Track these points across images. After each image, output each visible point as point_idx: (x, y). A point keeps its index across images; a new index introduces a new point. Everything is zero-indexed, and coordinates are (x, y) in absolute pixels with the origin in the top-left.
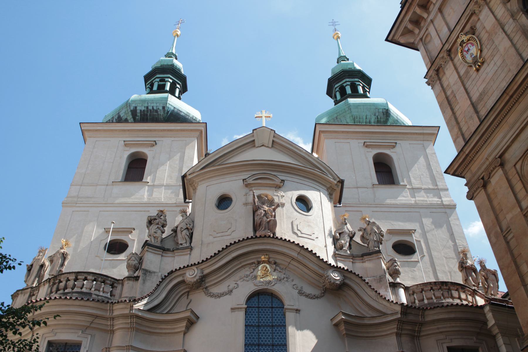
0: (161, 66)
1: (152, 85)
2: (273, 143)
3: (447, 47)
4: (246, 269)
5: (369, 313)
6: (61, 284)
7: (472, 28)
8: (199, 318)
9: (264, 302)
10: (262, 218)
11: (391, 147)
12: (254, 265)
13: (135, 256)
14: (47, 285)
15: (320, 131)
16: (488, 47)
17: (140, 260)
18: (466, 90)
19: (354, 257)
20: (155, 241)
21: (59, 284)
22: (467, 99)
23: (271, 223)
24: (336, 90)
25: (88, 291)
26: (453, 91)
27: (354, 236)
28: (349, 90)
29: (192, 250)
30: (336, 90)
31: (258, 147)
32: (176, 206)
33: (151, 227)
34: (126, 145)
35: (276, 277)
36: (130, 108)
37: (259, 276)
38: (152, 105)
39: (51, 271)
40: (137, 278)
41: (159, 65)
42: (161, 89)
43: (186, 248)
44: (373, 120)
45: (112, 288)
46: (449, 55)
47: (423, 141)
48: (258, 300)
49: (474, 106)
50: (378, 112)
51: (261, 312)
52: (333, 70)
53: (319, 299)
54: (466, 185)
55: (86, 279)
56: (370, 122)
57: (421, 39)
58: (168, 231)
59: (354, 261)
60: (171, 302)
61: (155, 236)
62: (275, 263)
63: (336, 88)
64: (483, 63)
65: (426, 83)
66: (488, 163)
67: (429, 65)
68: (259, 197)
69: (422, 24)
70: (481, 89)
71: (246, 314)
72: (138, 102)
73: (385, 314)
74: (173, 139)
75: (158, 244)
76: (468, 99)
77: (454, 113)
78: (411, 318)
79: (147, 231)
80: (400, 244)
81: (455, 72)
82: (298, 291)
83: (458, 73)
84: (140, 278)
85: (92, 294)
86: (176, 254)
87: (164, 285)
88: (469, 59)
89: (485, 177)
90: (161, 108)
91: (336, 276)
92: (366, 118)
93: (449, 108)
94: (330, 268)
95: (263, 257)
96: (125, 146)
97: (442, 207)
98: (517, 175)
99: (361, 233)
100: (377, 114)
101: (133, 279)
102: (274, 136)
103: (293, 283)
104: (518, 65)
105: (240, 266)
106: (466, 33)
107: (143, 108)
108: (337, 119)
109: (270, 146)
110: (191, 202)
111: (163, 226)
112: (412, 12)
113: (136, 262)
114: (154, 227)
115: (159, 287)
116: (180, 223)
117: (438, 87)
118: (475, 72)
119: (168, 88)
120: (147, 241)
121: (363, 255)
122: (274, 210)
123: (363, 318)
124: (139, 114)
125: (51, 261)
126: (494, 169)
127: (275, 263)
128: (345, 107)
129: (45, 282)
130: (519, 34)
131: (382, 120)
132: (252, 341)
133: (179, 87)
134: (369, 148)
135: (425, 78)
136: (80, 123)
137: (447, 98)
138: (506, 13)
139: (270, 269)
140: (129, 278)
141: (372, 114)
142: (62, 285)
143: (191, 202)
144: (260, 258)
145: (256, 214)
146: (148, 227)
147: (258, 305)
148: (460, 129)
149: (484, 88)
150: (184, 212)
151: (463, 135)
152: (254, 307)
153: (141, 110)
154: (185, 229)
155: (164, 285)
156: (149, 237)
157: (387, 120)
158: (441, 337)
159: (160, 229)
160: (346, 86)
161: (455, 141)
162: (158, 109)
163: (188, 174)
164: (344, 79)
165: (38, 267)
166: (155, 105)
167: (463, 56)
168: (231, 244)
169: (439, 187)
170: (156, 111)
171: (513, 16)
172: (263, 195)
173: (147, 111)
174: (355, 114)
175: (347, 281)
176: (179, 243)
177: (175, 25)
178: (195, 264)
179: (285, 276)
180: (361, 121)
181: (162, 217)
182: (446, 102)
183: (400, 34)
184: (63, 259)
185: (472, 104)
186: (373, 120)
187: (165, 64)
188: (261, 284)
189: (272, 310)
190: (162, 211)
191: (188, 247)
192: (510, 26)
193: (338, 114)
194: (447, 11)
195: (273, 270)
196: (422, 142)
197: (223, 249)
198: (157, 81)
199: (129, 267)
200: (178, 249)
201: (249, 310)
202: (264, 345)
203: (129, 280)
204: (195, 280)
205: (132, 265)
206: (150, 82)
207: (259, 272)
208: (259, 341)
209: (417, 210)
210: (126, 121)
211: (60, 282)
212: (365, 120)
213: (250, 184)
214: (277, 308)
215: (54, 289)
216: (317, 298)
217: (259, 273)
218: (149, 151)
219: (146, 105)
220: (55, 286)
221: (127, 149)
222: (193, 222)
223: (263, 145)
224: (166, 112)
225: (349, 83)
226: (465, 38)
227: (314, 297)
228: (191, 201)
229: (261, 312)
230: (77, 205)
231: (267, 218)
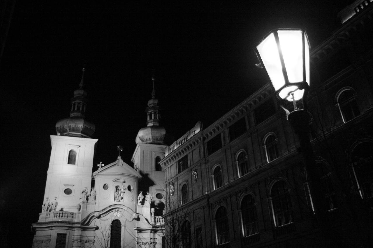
56: (158, 139)
62: (120, 211)
78: (154, 229)
90: (81, 127)
107: (73, 126)
109: (121, 165)
111: (87, 193)
114: (84, 193)
186: (159, 138)
207: (115, 214)
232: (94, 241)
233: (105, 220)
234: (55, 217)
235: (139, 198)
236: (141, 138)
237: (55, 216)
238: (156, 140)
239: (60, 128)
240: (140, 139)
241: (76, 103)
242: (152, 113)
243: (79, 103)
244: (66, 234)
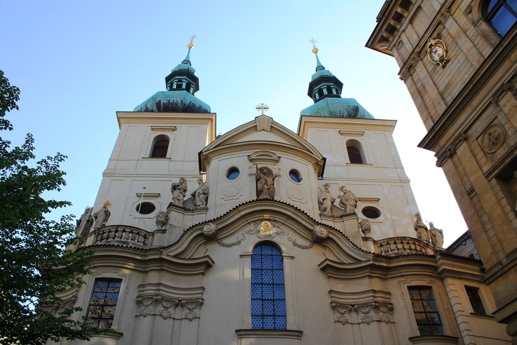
0: (179, 70)
1: (172, 84)
2: (271, 129)
3: (418, 50)
4: (252, 225)
5: (347, 260)
6: (104, 235)
7: (439, 34)
8: (214, 262)
9: (265, 251)
10: (264, 186)
11: (360, 135)
12: (258, 222)
13: (163, 214)
14: (93, 236)
15: (305, 121)
16: (453, 48)
17: (167, 217)
18: (434, 82)
19: (334, 217)
20: (178, 202)
21: (103, 235)
22: (435, 89)
23: (271, 189)
24: (316, 92)
25: (125, 240)
26: (422, 83)
27: (334, 201)
28: (325, 92)
29: (208, 210)
30: (316, 92)
31: (260, 131)
32: (193, 177)
33: (175, 192)
34: (152, 129)
35: (275, 232)
36: (155, 101)
37: (261, 231)
38: (173, 99)
39: (96, 224)
40: (165, 231)
41: (177, 69)
42: (179, 87)
43: (203, 209)
44: (345, 115)
45: (145, 238)
46: (419, 56)
47: (385, 131)
48: (261, 249)
49: (441, 95)
51: (263, 259)
52: (313, 76)
53: (309, 249)
54: (435, 156)
55: (124, 231)
57: (394, 45)
58: (188, 195)
59: (334, 221)
60: (192, 250)
61: (178, 198)
62: (275, 221)
63: (315, 90)
64: (448, 61)
65: (400, 78)
66: (454, 138)
67: (402, 65)
68: (261, 169)
69: (395, 34)
70: (446, 82)
71: (252, 260)
72: (162, 97)
73: (359, 261)
74: (190, 125)
75: (181, 205)
76: (436, 89)
77: (423, 101)
80: (367, 210)
81: (424, 68)
82: (292, 242)
83: (427, 70)
84: (167, 232)
85: (129, 242)
86: (195, 213)
87: (186, 236)
88: (437, 58)
89: (451, 149)
90: (180, 102)
92: (340, 113)
93: (419, 97)
94: (318, 225)
95: (265, 215)
96: (152, 130)
97: (400, 181)
98: (478, 146)
99: (339, 199)
100: (348, 110)
101: (161, 232)
102: (272, 123)
103: (289, 236)
104: (479, 61)
105: (247, 222)
106: (434, 38)
107: (166, 102)
108: (317, 113)
109: (269, 131)
110: (206, 174)
111: (185, 191)
112: (387, 24)
113: (164, 218)
114: (177, 192)
115: (182, 238)
116: (198, 189)
117: (409, 80)
118: (442, 69)
119: (184, 86)
120: (171, 203)
121: (342, 217)
122: (273, 179)
123: (343, 264)
125: (96, 218)
126: (459, 142)
127: (275, 221)
128: (324, 104)
129: (92, 233)
130: (479, 37)
131: (352, 115)
132: (257, 281)
133: (193, 86)
134: (343, 135)
135: (398, 74)
136: (116, 112)
137: (418, 89)
138: (468, 22)
139: (270, 226)
140: (158, 231)
141: (345, 109)
142: (105, 235)
143: (206, 174)
144: (263, 217)
145: (259, 182)
146: (172, 192)
147: (261, 253)
148: (429, 113)
149: (449, 81)
150: (201, 180)
151: (431, 117)
152: (258, 255)
153: (164, 103)
154: (202, 194)
155: (186, 236)
156: (173, 200)
157: (356, 115)
158: (402, 279)
159: (182, 194)
160: (323, 88)
161: (425, 122)
162: (178, 102)
163: (203, 151)
164: (322, 83)
165: (85, 222)
166: (175, 99)
167: (431, 56)
168: (240, 205)
169: (397, 167)
170: (176, 104)
171: (475, 24)
172: (264, 167)
173: (169, 104)
174: (331, 109)
175: (330, 236)
176: (197, 205)
178: (211, 221)
179: (282, 230)
180: (336, 115)
181: (183, 184)
182: (417, 93)
183: (377, 41)
184: (105, 215)
185: (439, 93)
186: (345, 115)
187: (182, 68)
188: (263, 237)
189: (272, 257)
191: (204, 207)
192: (472, 31)
193: (318, 109)
194: (416, 22)
195: (272, 226)
196: (383, 132)
197: (233, 209)
198: (176, 82)
199: (158, 222)
200: (196, 209)
201: (254, 257)
202: (266, 284)
203: (159, 232)
204: (212, 233)
205: (160, 221)
206: (170, 83)
208: (262, 281)
209: (381, 184)
210: (152, 111)
211: (104, 233)
212: (339, 114)
213: (253, 159)
214: (276, 255)
216: (307, 248)
217: (262, 228)
218: (171, 134)
219: (168, 99)
220: (100, 237)
221: (154, 132)
223: (263, 130)
224: (184, 105)
226: (433, 42)
227: (305, 247)
228: (205, 173)
229: (263, 259)
230: (115, 175)
231: (267, 186)
232: (203, 300)
233: (233, 244)
235: (324, 200)
242: (322, 88)
243: (180, 81)
244: (120, 281)
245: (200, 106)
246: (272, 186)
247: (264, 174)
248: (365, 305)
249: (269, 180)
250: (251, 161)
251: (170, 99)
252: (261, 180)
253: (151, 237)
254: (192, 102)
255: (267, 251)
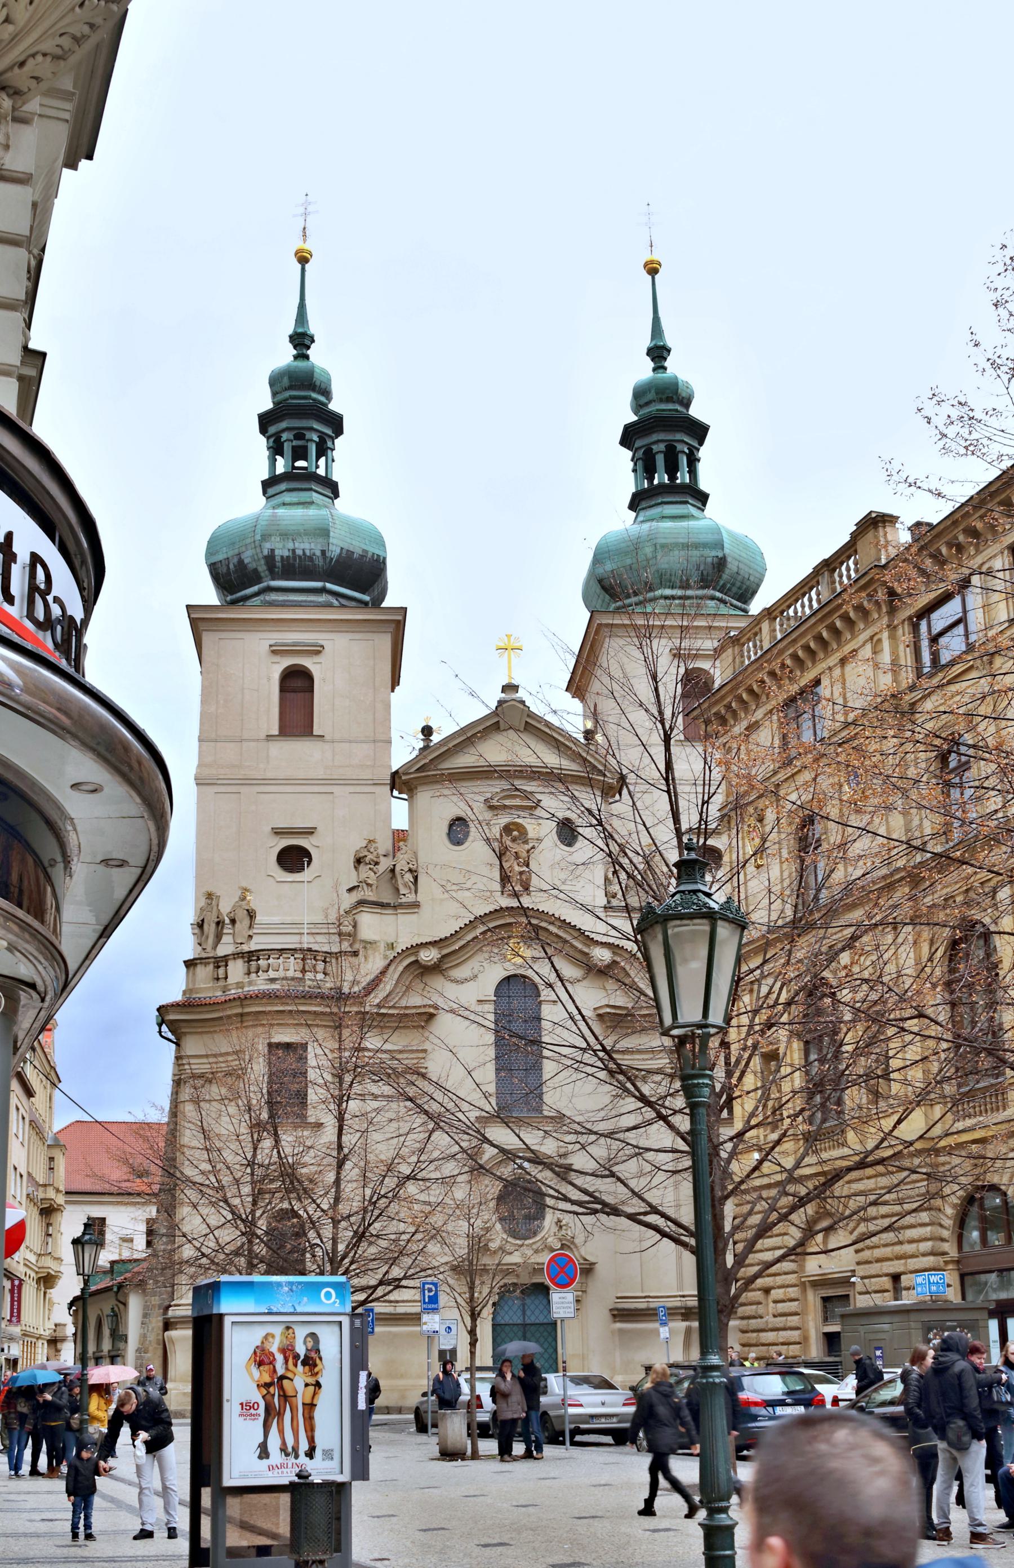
38: (302, 546)
50: (705, 563)
58: (381, 868)
79: (354, 873)
86: (399, 911)
90: (318, 553)
91: (602, 956)
100: (702, 568)
107: (286, 553)
111: (377, 864)
113: (351, 928)
114: (362, 867)
124: (279, 564)
131: (709, 578)
145: (504, 859)
153: (282, 557)
162: (314, 554)
165: (214, 926)
170: (310, 559)
174: (663, 566)
177: (295, 216)
190: (370, 841)
215: (253, 969)
219: (291, 546)
221: (277, 658)
222: (415, 854)
223: (511, 728)
224: (328, 560)
225: (662, 447)
234: (249, 973)
236: (606, 583)
237: (249, 969)
238: (681, 587)
239: (228, 566)
240: (603, 588)
241: (285, 436)
242: (655, 448)
245: (364, 551)
246: (525, 869)
247: (514, 840)
248: (659, 1071)
249: (522, 849)
250: (492, 808)
251: (297, 545)
252: (508, 853)
253: (334, 960)
254: (346, 546)
255: (516, 988)
